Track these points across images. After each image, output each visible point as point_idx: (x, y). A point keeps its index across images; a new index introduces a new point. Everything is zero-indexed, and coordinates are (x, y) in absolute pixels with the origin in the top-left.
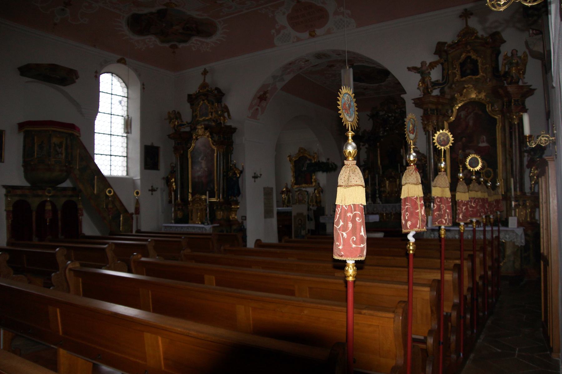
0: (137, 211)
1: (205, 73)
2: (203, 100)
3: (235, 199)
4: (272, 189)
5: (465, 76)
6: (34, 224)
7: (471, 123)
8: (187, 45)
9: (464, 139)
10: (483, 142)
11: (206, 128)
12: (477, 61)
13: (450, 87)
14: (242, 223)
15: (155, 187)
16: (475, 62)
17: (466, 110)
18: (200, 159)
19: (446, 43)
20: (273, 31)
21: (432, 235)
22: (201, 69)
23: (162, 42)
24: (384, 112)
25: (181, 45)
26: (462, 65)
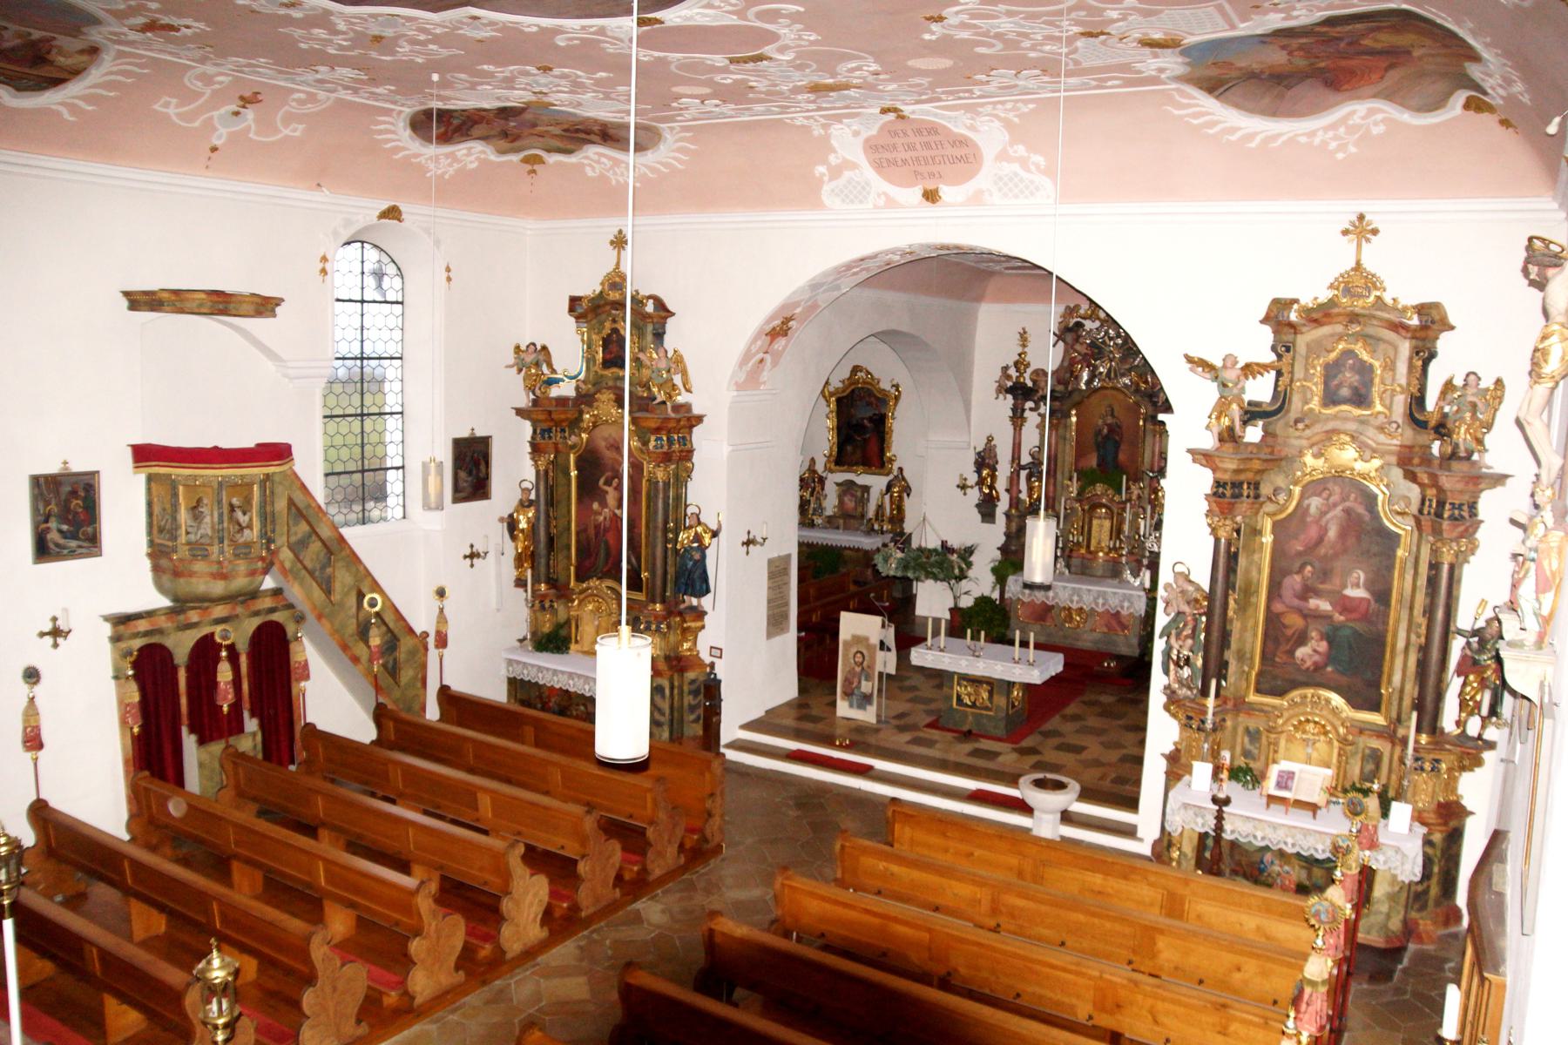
0: (442, 641)
1: (619, 242)
3: (694, 601)
4: (789, 556)
5: (1335, 403)
6: (184, 701)
7: (1332, 533)
9: (1309, 568)
10: (1357, 585)
14: (712, 665)
15: (479, 548)
16: (1365, 370)
18: (602, 481)
19: (1296, 301)
20: (821, 169)
21: (1200, 820)
22: (610, 226)
23: (502, 152)
24: (1097, 324)
25: (553, 159)
26: (1331, 371)
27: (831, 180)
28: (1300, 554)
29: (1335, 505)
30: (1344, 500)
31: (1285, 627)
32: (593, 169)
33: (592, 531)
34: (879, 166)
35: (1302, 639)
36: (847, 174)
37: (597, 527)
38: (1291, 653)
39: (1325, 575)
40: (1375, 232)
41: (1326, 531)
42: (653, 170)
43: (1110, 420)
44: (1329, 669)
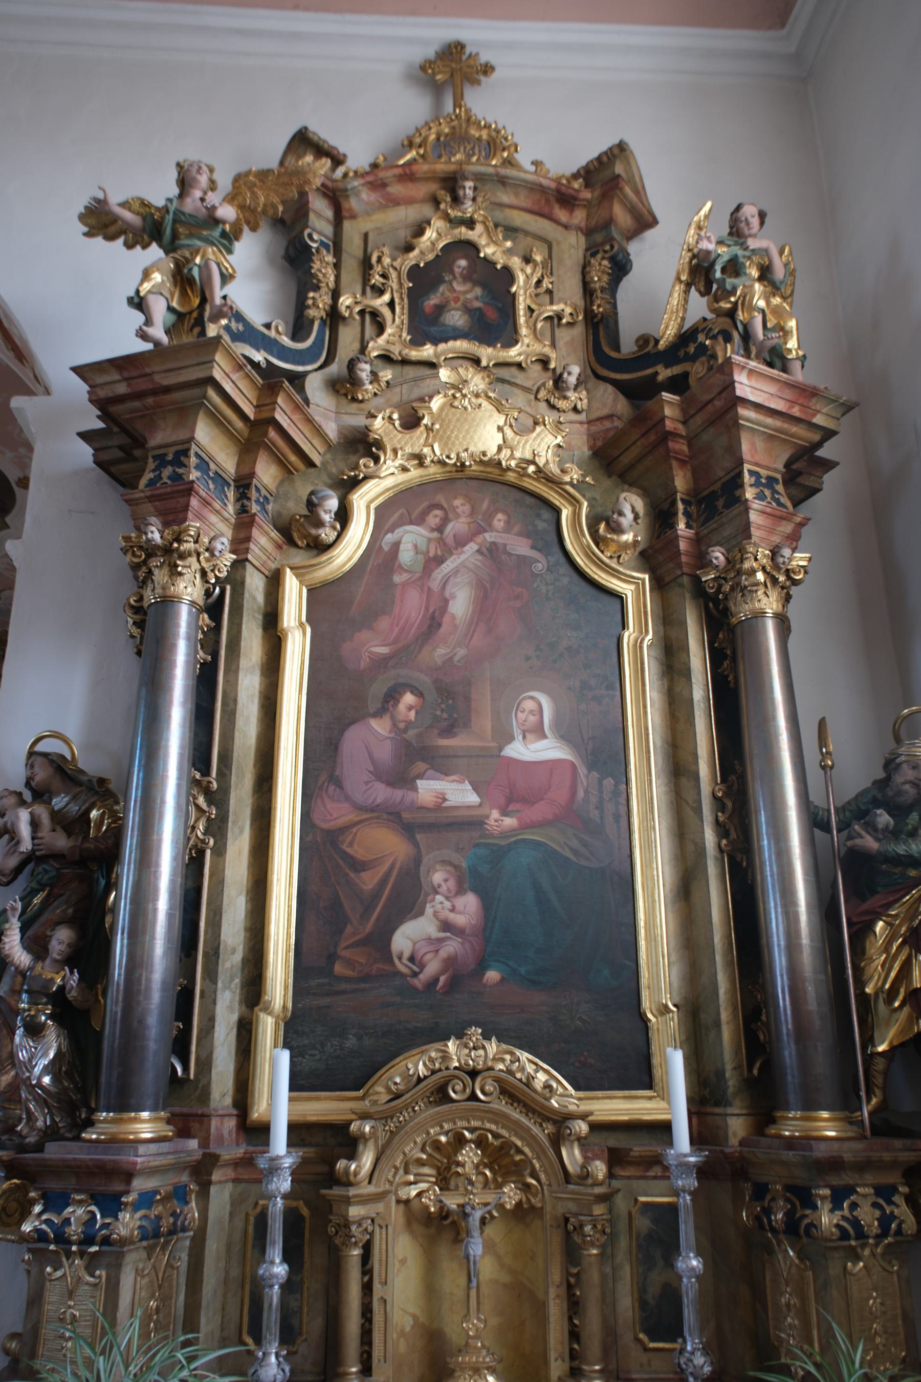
7: (460, 604)
9: (409, 698)
10: (539, 731)
12: (508, 275)
13: (345, 387)
17: (434, 518)
28: (381, 663)
29: (460, 542)
30: (481, 530)
31: (359, 866)
35: (407, 899)
38: (379, 942)
39: (451, 703)
40: (488, 69)
41: (445, 603)
44: (492, 975)
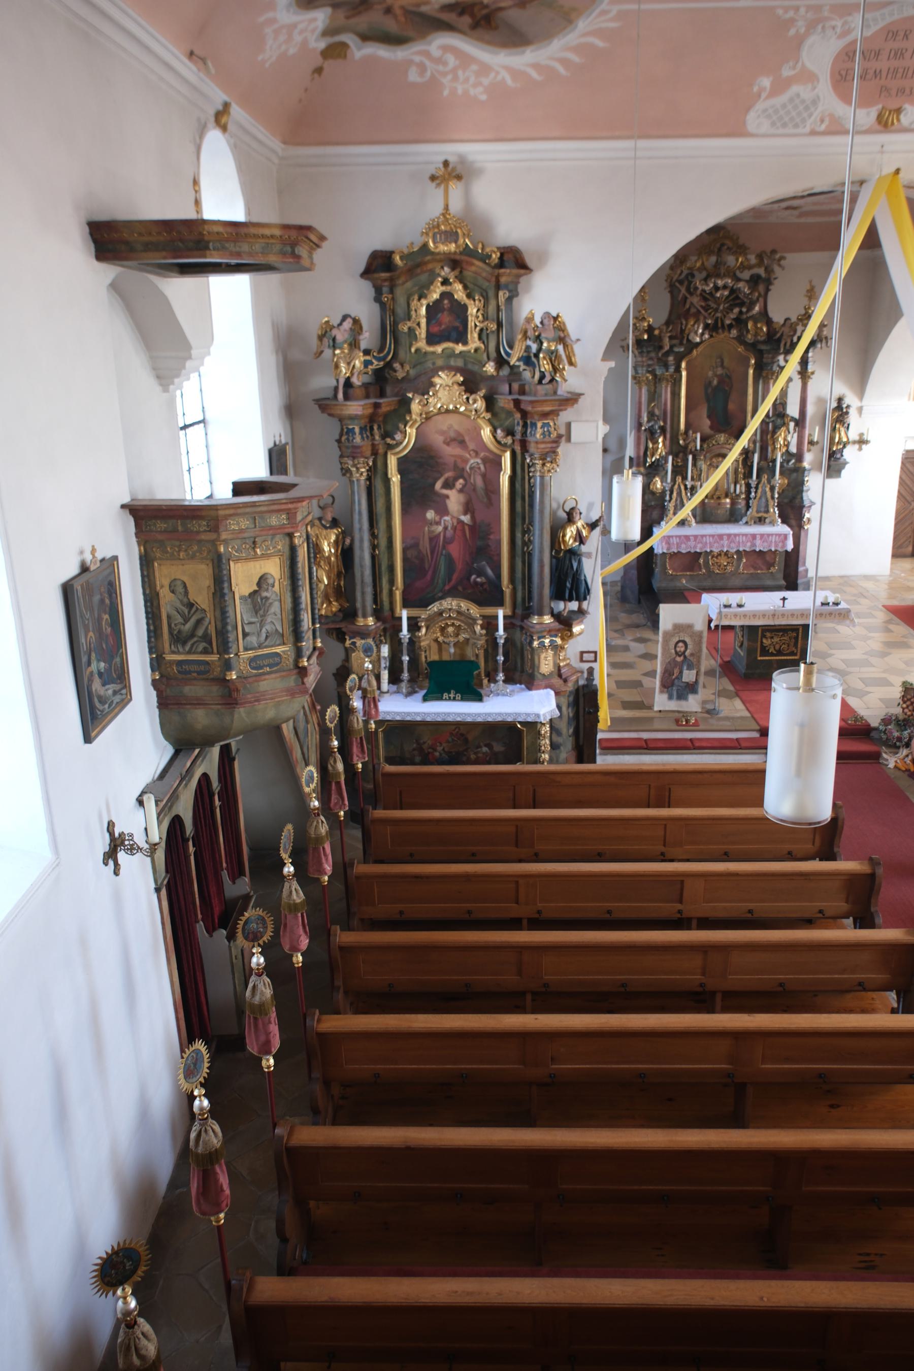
2: (445, 282)
3: (574, 605)
8: (399, 54)
11: (470, 386)
14: (591, 671)
18: (438, 485)
20: (766, 82)
27: (767, 98)
32: (422, 68)
33: (425, 546)
34: (841, 79)
36: (795, 89)
37: (433, 539)
42: (515, 73)
43: (719, 371)
